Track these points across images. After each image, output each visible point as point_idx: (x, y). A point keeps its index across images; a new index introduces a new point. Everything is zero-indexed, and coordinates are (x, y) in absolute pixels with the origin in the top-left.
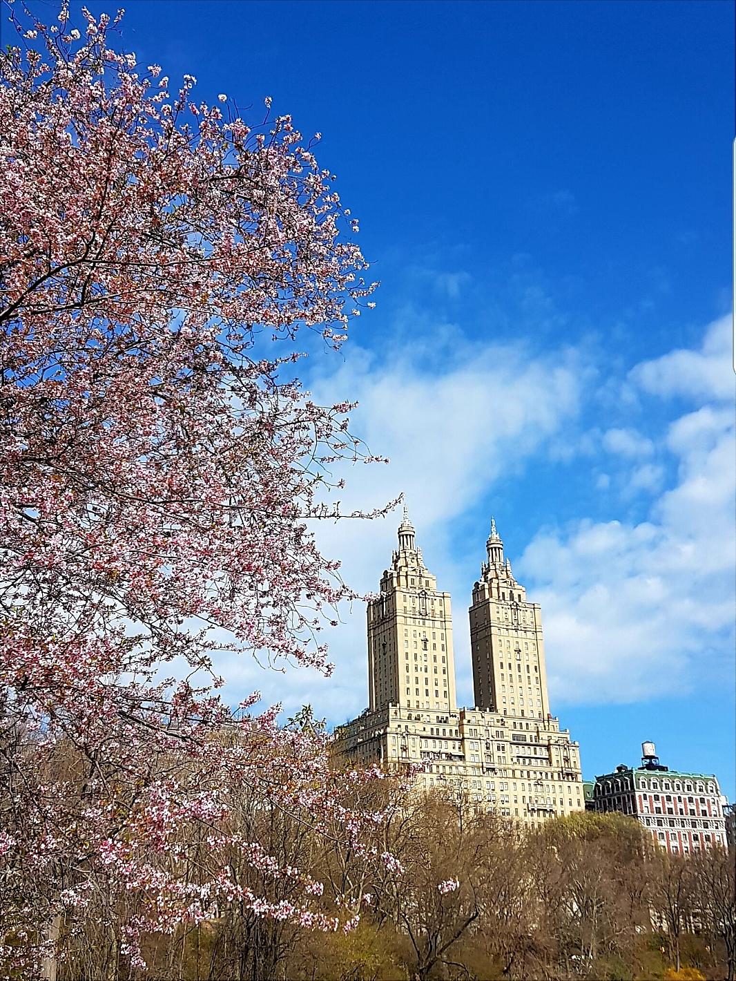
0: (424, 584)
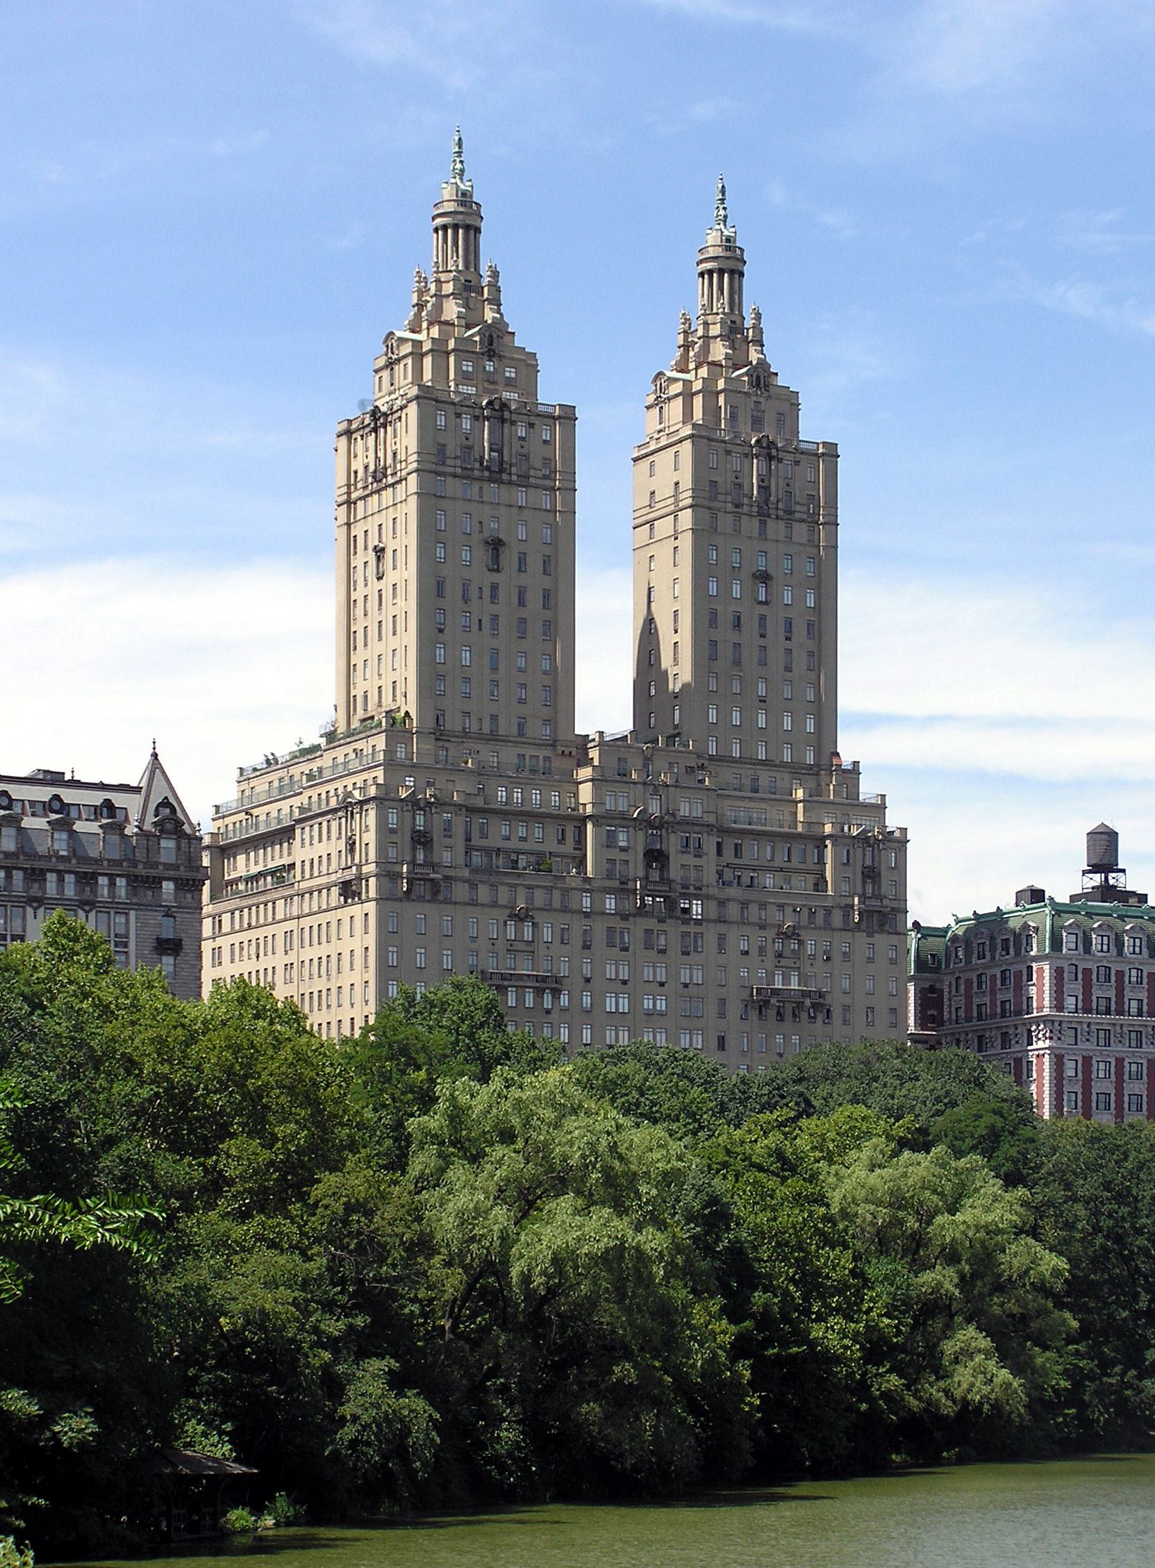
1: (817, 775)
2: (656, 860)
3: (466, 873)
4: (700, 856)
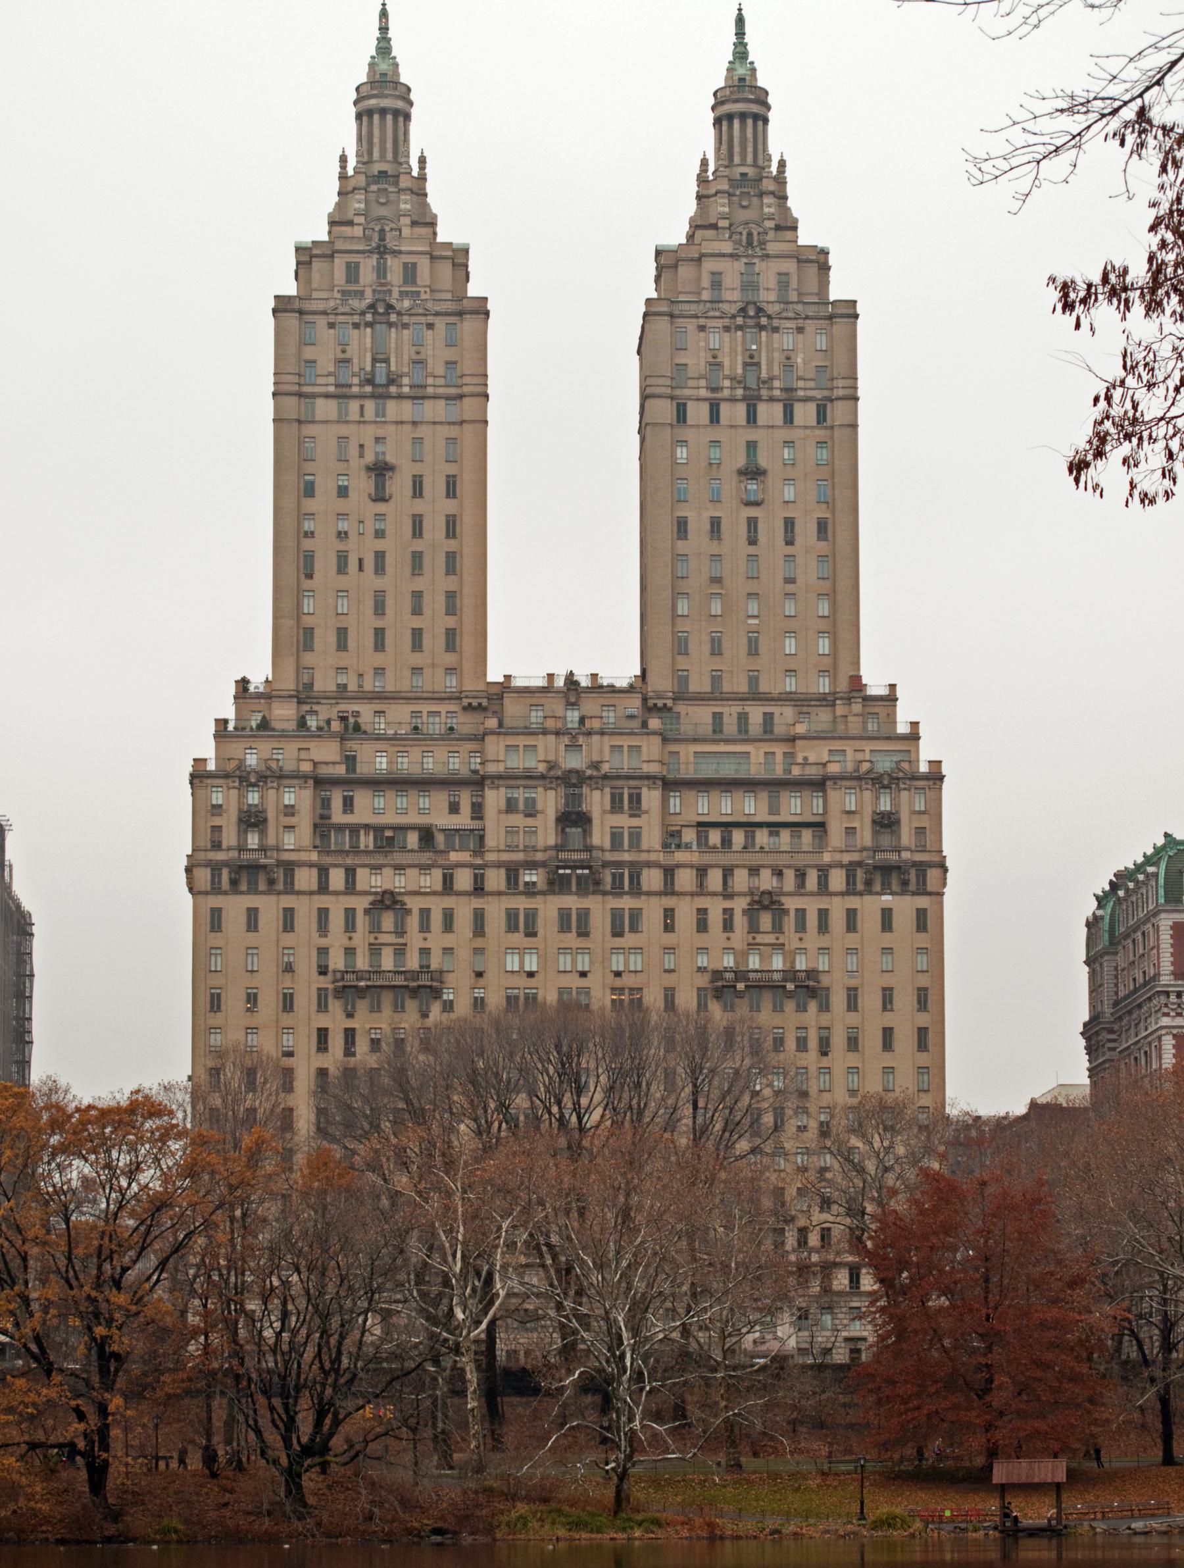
0: (395, 275)
1: (834, 705)
2: (575, 824)
3: (314, 856)
4: (639, 816)
